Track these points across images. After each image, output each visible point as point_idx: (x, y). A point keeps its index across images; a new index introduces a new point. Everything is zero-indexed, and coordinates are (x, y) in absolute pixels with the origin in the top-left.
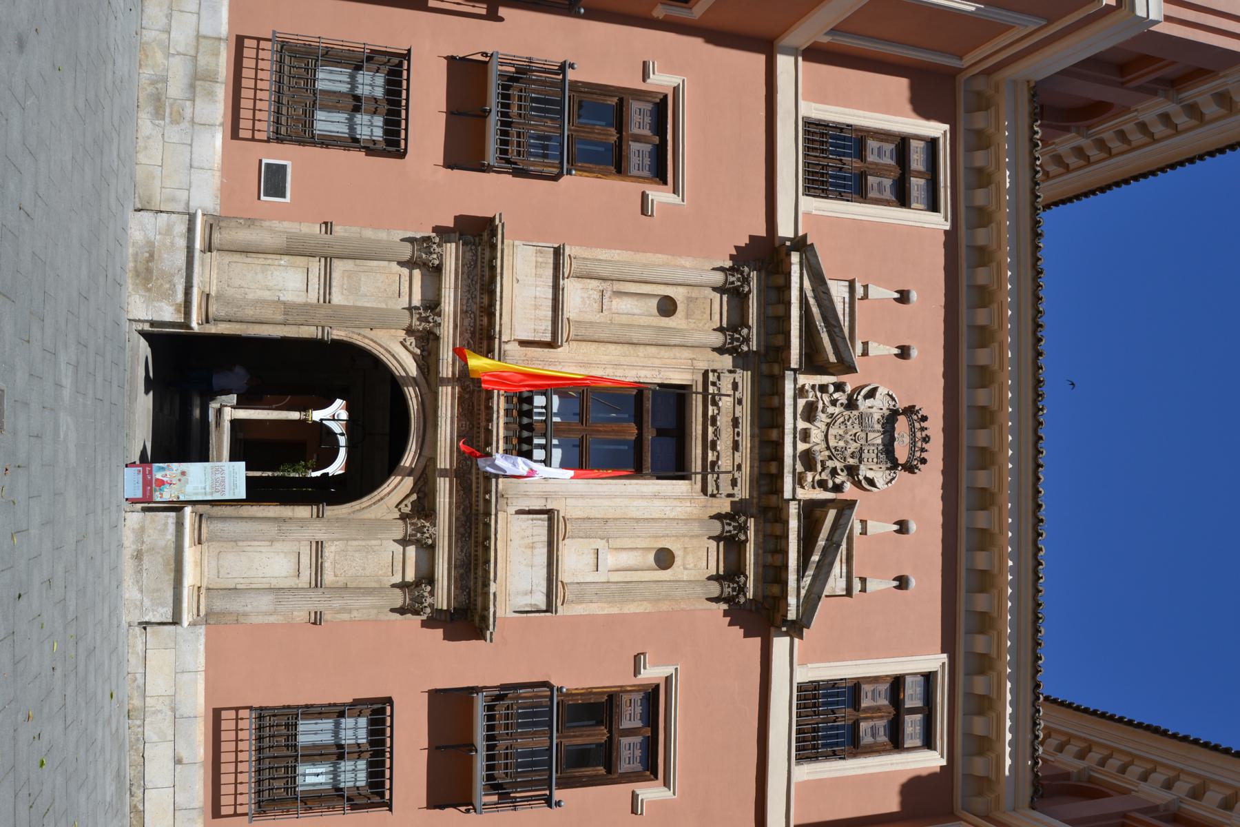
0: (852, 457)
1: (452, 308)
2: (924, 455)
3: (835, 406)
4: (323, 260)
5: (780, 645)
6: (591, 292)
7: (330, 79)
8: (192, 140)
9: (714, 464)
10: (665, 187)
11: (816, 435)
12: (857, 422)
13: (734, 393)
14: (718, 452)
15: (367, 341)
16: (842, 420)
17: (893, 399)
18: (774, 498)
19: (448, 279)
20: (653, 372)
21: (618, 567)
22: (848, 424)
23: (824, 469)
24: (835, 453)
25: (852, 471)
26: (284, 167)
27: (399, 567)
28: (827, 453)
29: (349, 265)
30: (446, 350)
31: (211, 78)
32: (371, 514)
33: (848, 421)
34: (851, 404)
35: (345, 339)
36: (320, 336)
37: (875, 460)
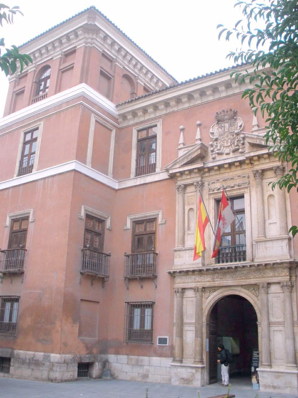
0: (233, 135)
1: (194, 284)
2: (229, 110)
3: (217, 146)
4: (184, 326)
6: (188, 238)
7: (137, 326)
8: (153, 366)
10: (157, 218)
11: (227, 151)
12: (222, 137)
13: (216, 183)
14: (234, 185)
15: (206, 311)
16: (221, 142)
17: (214, 125)
19: (186, 286)
20: (211, 213)
22: (223, 140)
24: (233, 142)
25: (238, 134)
26: (159, 339)
27: (277, 295)
28: (233, 145)
29: (185, 318)
30: (206, 285)
31: (137, 361)
32: (260, 306)
33: (222, 140)
34: (216, 140)
35: (206, 318)
36: (205, 326)
37: (234, 127)
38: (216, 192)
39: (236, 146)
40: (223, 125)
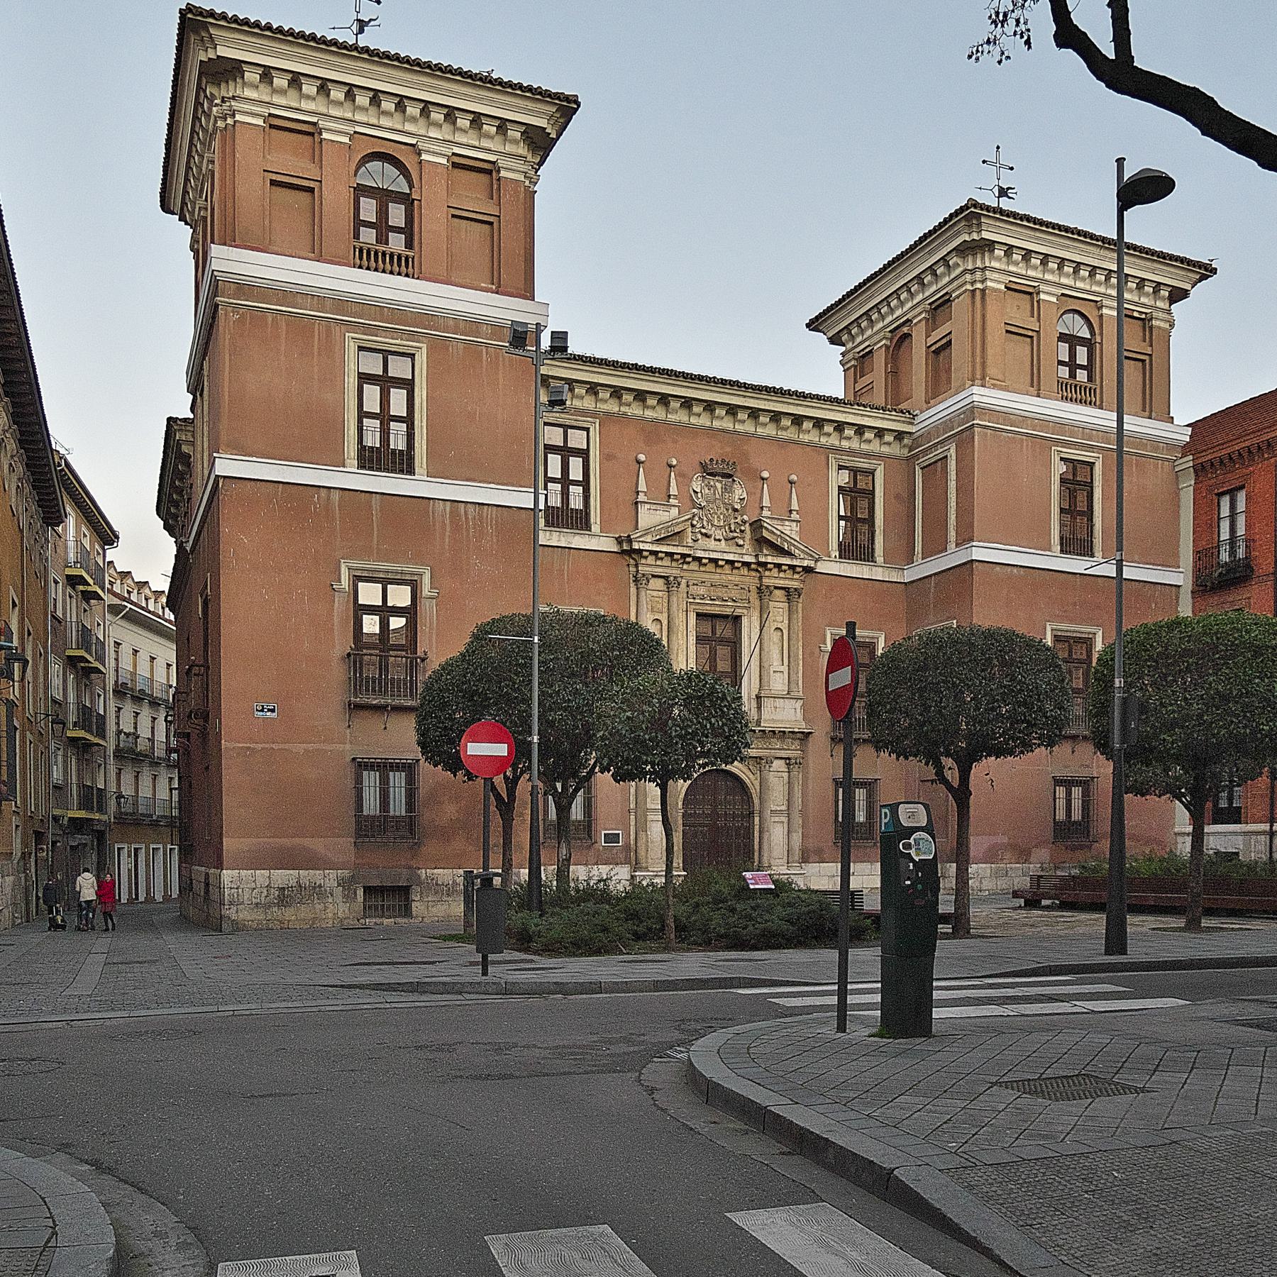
5: (821, 567)
9: (734, 601)
18: (753, 566)
21: (780, 659)
23: (735, 531)
25: (736, 510)
38: (699, 601)
39: (731, 532)
40: (712, 483)
